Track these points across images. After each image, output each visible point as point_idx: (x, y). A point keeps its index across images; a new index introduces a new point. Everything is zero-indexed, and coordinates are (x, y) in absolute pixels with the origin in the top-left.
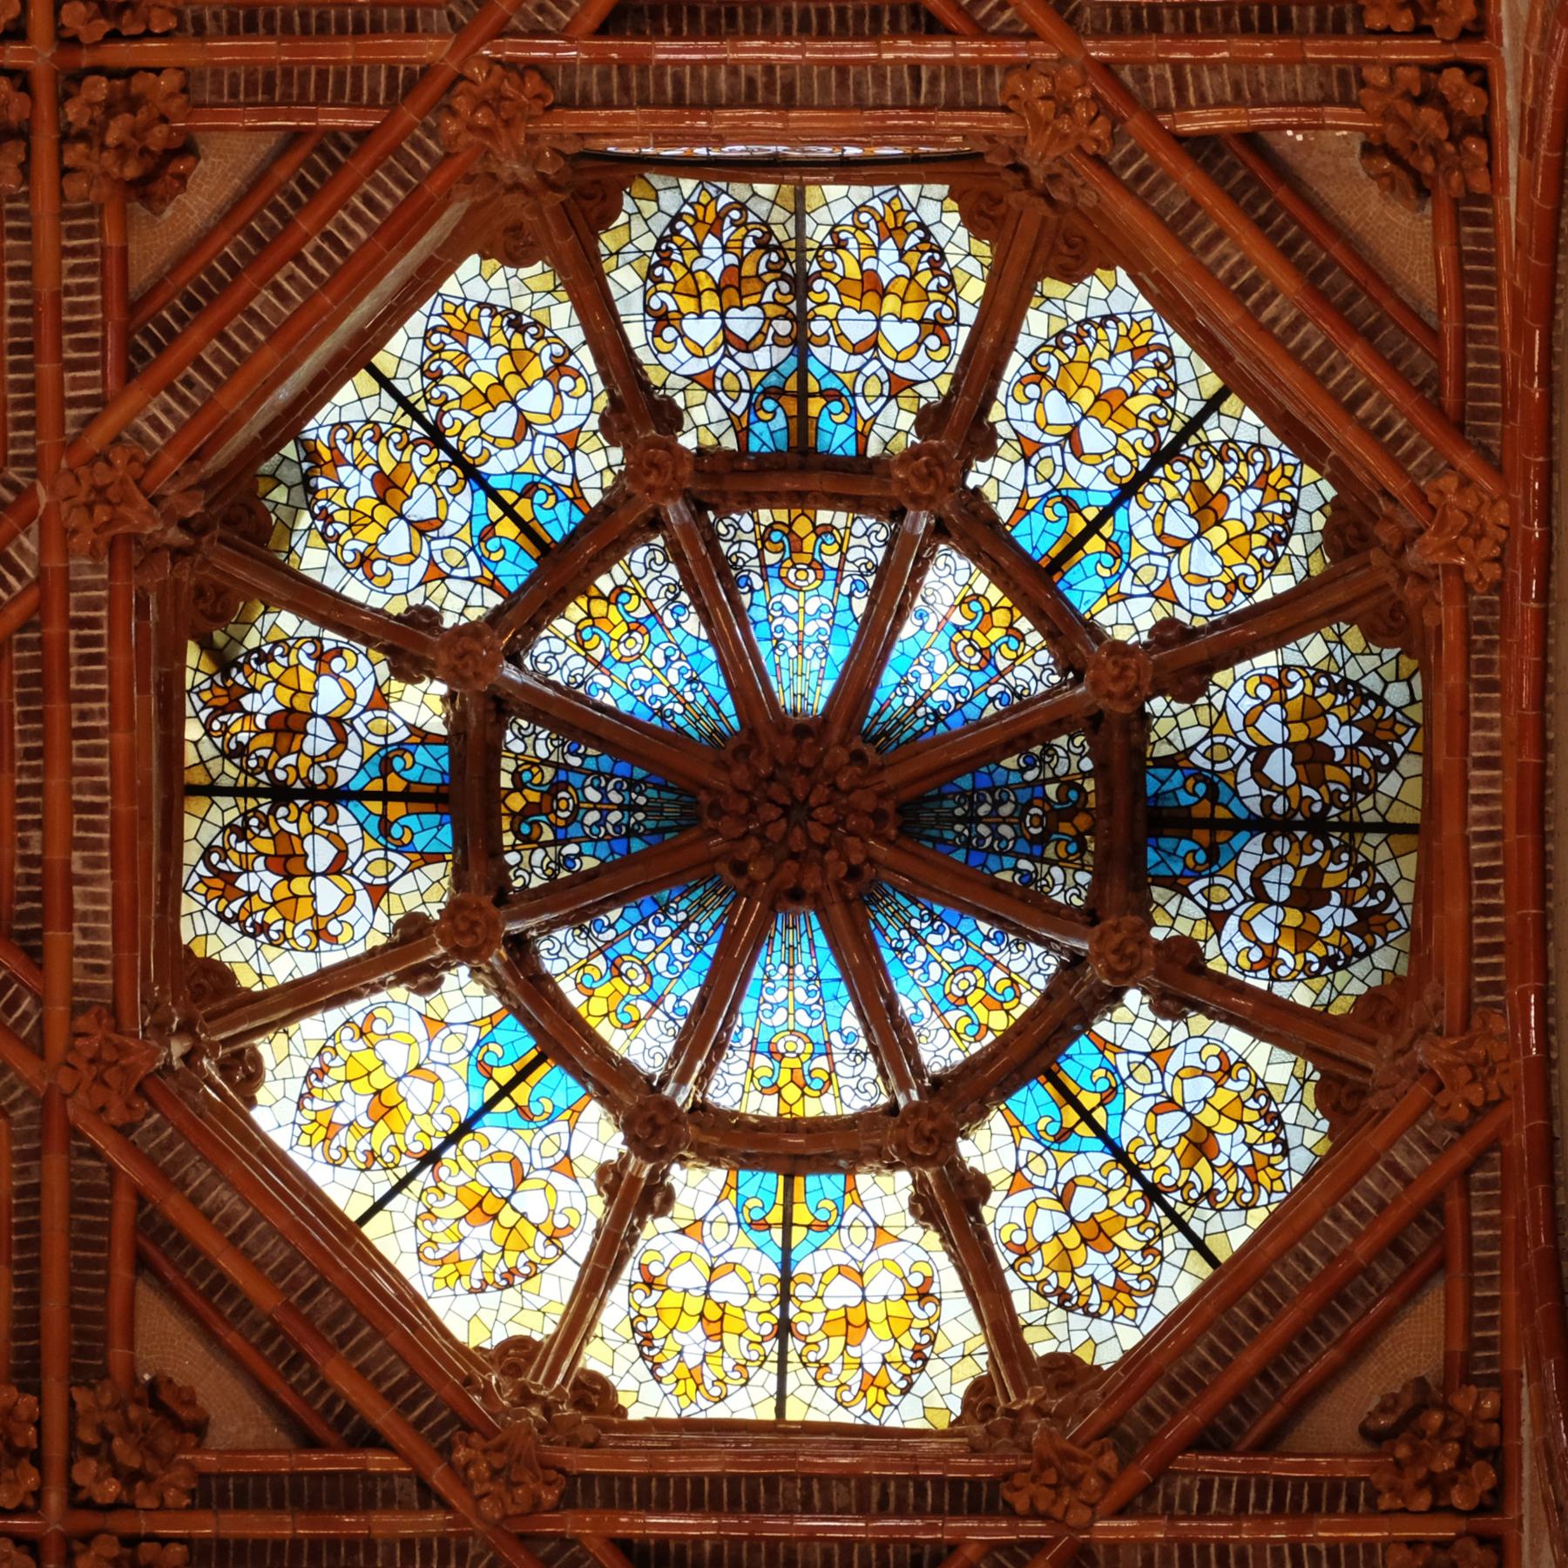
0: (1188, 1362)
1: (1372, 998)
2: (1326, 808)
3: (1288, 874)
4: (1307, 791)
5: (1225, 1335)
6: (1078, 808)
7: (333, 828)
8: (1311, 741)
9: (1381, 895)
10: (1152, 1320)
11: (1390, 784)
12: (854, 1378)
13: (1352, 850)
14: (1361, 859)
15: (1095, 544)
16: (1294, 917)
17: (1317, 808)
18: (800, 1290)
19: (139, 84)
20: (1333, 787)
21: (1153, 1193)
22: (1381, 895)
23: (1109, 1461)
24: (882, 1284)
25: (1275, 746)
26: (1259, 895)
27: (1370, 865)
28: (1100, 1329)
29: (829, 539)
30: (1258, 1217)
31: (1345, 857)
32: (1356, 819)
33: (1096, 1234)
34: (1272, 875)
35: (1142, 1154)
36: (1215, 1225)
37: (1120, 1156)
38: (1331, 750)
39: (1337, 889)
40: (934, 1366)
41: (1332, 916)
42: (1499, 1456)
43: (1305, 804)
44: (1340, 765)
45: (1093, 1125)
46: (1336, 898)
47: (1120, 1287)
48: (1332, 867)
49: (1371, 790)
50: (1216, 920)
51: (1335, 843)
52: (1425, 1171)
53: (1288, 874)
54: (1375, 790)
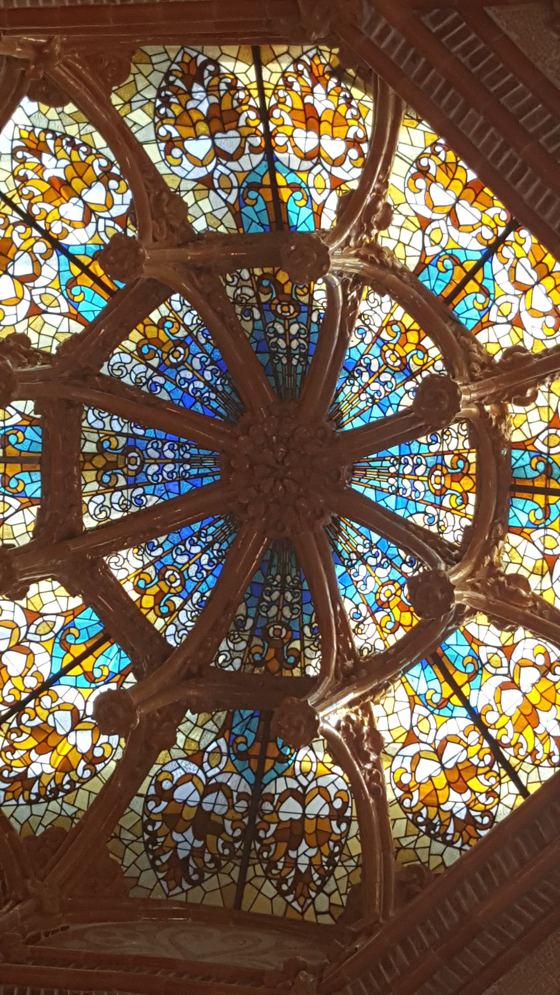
2: (260, 840)
4: (273, 827)
7: (247, 151)
8: (303, 835)
9: (195, 877)
13: (229, 858)
14: (223, 863)
15: (448, 690)
17: (262, 834)
20: (273, 847)
22: (195, 877)
25: (304, 807)
27: (219, 868)
29: (459, 501)
31: (227, 852)
32: (251, 862)
38: (296, 848)
39: (205, 846)
43: (265, 825)
44: (286, 854)
45: (71, 666)
46: (198, 844)
48: (221, 842)
49: (267, 876)
51: (237, 845)
54: (267, 878)
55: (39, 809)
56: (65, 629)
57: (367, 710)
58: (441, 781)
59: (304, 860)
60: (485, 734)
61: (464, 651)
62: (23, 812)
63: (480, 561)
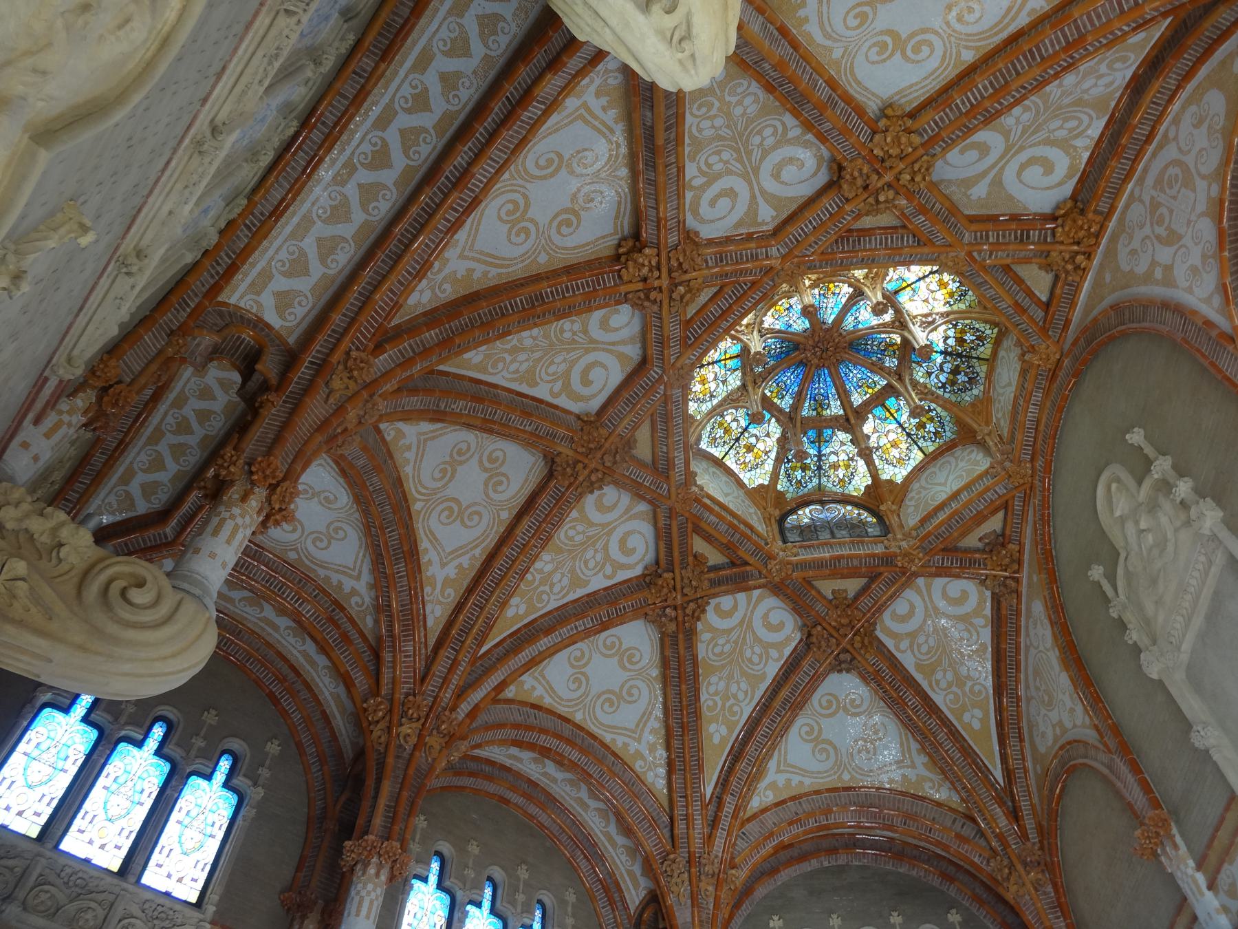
0: (940, 531)
1: (973, 405)
3: (950, 366)
5: (949, 525)
6: (894, 344)
10: (910, 468)
11: (981, 349)
12: (837, 480)
15: (909, 289)
16: (951, 377)
18: (823, 458)
19: (691, 284)
21: (909, 435)
23: (921, 555)
24: (843, 457)
26: (942, 370)
28: (897, 470)
30: (936, 445)
33: (894, 445)
34: (946, 365)
35: (906, 425)
36: (925, 444)
37: (901, 425)
40: (856, 478)
41: (962, 378)
42: (1020, 562)
47: (900, 458)
50: (929, 374)
52: (1004, 494)
53: (950, 366)
55: (947, 429)
56: (880, 419)
57: (915, 317)
58: (944, 291)
59: (972, 338)
60: (928, 276)
61: (894, 283)
62: (949, 434)
63: (863, 284)
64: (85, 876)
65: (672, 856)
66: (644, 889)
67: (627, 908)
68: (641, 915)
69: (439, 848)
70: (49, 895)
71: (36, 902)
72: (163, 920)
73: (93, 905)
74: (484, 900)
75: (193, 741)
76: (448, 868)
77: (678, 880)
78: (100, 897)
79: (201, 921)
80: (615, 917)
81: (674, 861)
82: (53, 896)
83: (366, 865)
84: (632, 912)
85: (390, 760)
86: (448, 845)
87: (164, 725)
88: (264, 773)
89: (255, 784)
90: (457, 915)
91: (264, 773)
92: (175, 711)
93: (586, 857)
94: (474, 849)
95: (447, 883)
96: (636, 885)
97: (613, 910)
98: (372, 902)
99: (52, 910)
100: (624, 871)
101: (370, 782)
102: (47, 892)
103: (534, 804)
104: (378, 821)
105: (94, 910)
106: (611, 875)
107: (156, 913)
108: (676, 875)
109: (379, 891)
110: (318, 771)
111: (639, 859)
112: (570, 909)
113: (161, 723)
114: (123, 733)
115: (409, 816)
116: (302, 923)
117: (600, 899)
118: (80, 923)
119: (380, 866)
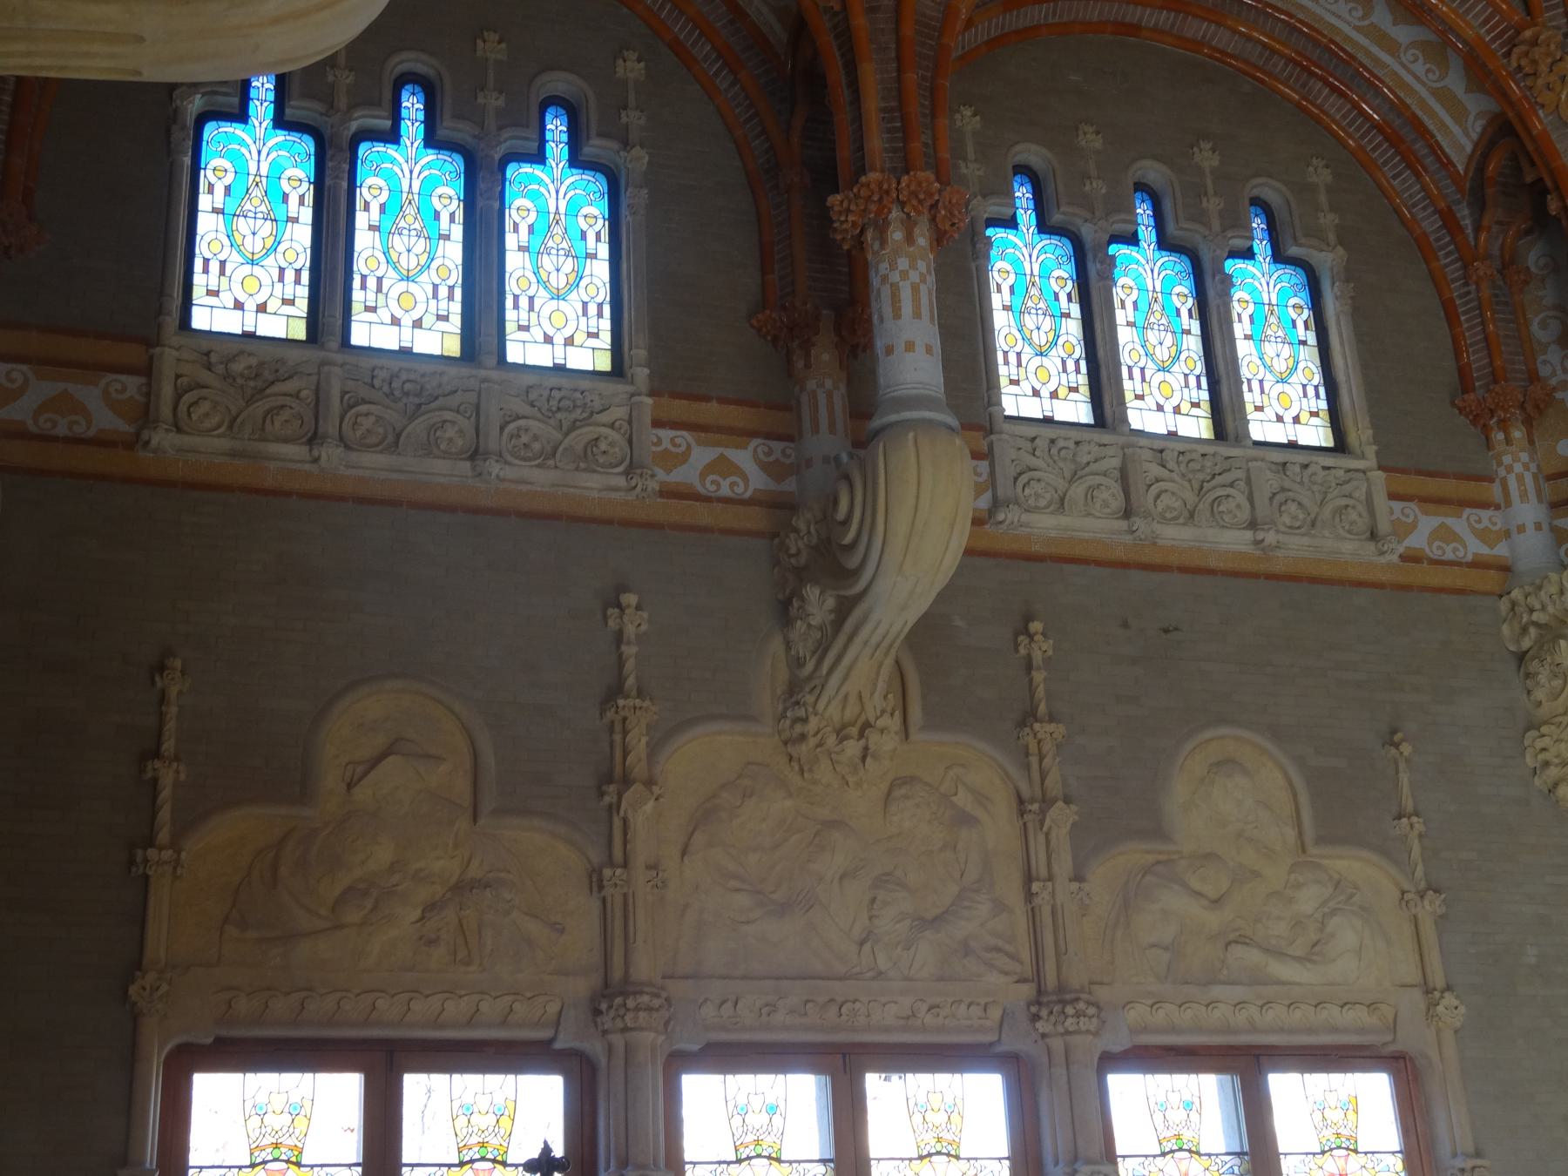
64: (412, 377)
65: (1528, 34)
66: (1478, 116)
67: (1446, 164)
68: (1481, 169)
69: (1021, 158)
70: (372, 419)
71: (358, 433)
72: (567, 410)
73: (448, 415)
74: (1141, 229)
75: (481, 100)
76: (1049, 190)
77: (1552, 78)
78: (454, 401)
79: (632, 395)
80: (1424, 188)
81: (1534, 42)
82: (379, 419)
83: (882, 229)
84: (1461, 169)
85: (860, 21)
86: (1034, 147)
87: (417, 89)
88: (633, 119)
89: (626, 144)
90: (1093, 269)
91: (633, 119)
92: (424, 57)
93: (1334, 89)
94: (1091, 140)
95: (1056, 218)
96: (1459, 114)
97: (1418, 175)
98: (915, 289)
99: (390, 439)
100: (1424, 93)
101: (836, 74)
102: (367, 414)
103: (1195, 16)
104: (876, 142)
105: (453, 423)
106: (1400, 108)
107: (554, 403)
108: (1544, 68)
109: (922, 266)
110: (732, 85)
111: (1456, 63)
112: (1323, 198)
113: (409, 87)
114: (354, 126)
115: (933, 115)
116: (808, 354)
117: (1385, 163)
118: (443, 447)
119: (909, 226)
